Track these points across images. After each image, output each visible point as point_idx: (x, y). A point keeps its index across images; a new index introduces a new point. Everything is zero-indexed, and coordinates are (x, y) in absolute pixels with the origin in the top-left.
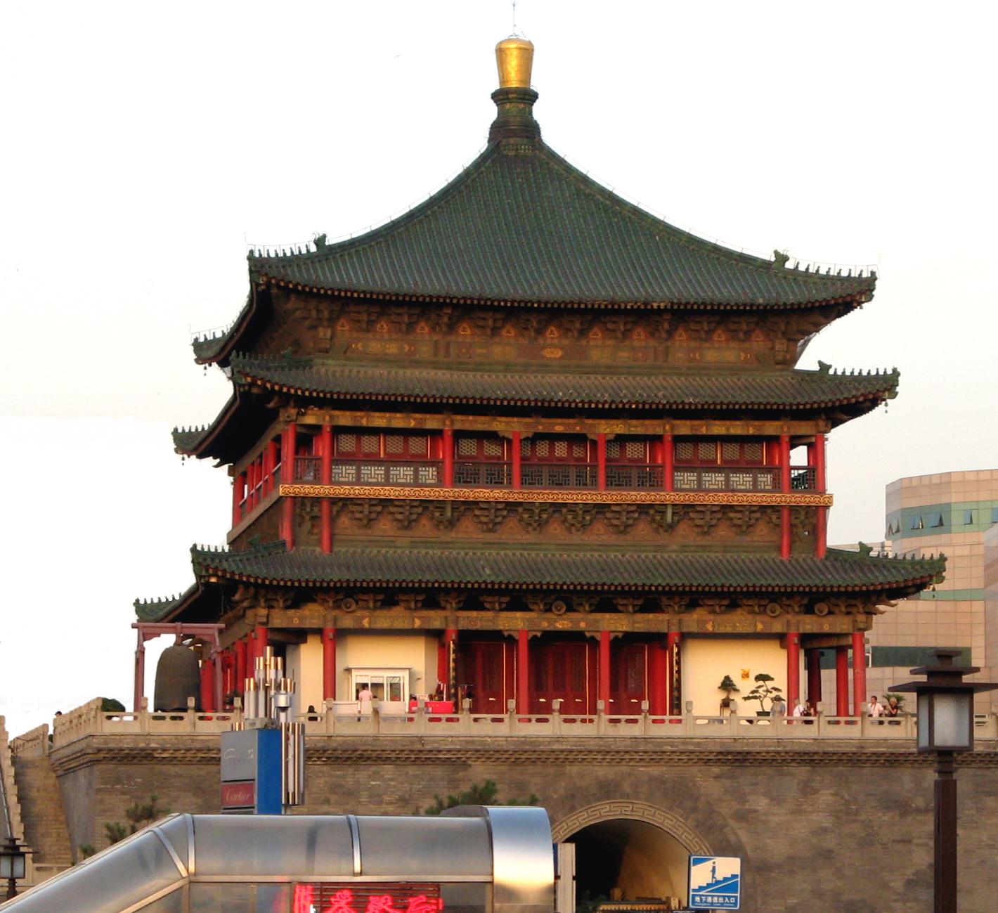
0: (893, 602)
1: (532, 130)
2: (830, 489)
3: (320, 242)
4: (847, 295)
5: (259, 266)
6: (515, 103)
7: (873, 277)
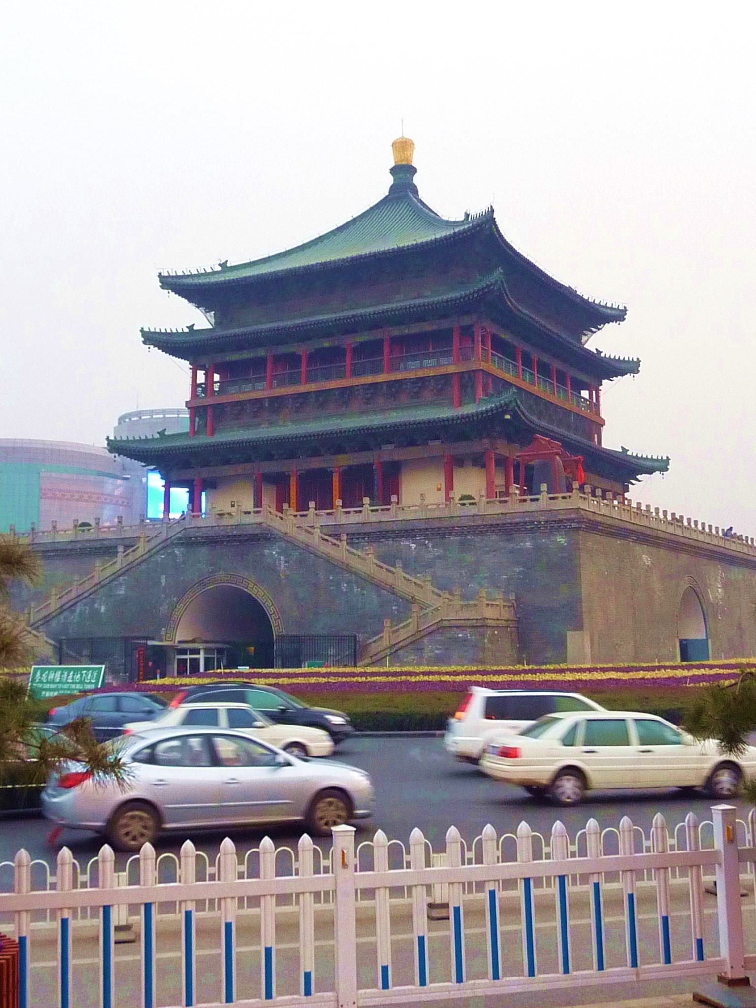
0: (639, 477)
1: (415, 190)
2: (603, 416)
3: (467, 215)
4: (618, 316)
5: (488, 221)
6: (404, 174)
7: (625, 310)
